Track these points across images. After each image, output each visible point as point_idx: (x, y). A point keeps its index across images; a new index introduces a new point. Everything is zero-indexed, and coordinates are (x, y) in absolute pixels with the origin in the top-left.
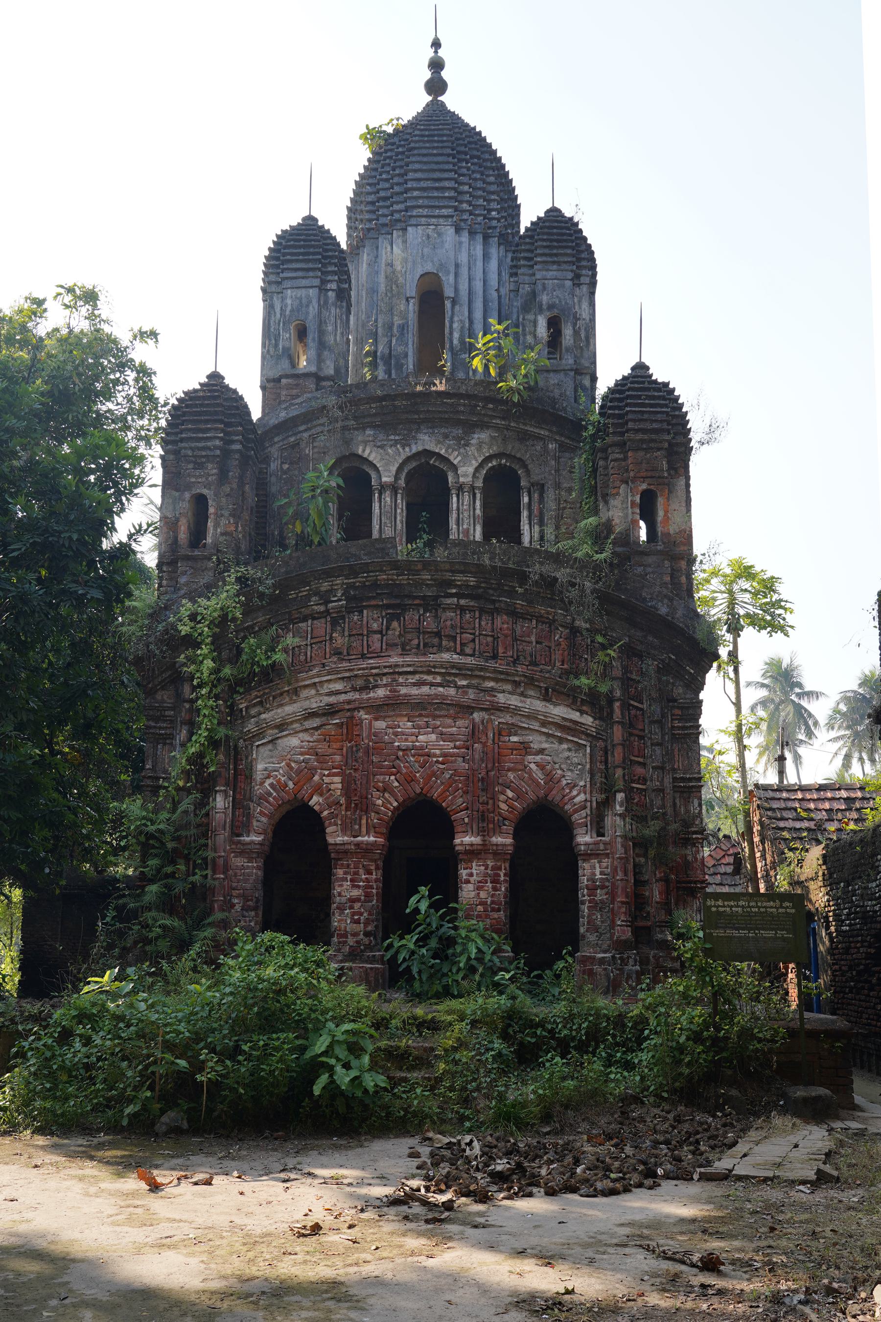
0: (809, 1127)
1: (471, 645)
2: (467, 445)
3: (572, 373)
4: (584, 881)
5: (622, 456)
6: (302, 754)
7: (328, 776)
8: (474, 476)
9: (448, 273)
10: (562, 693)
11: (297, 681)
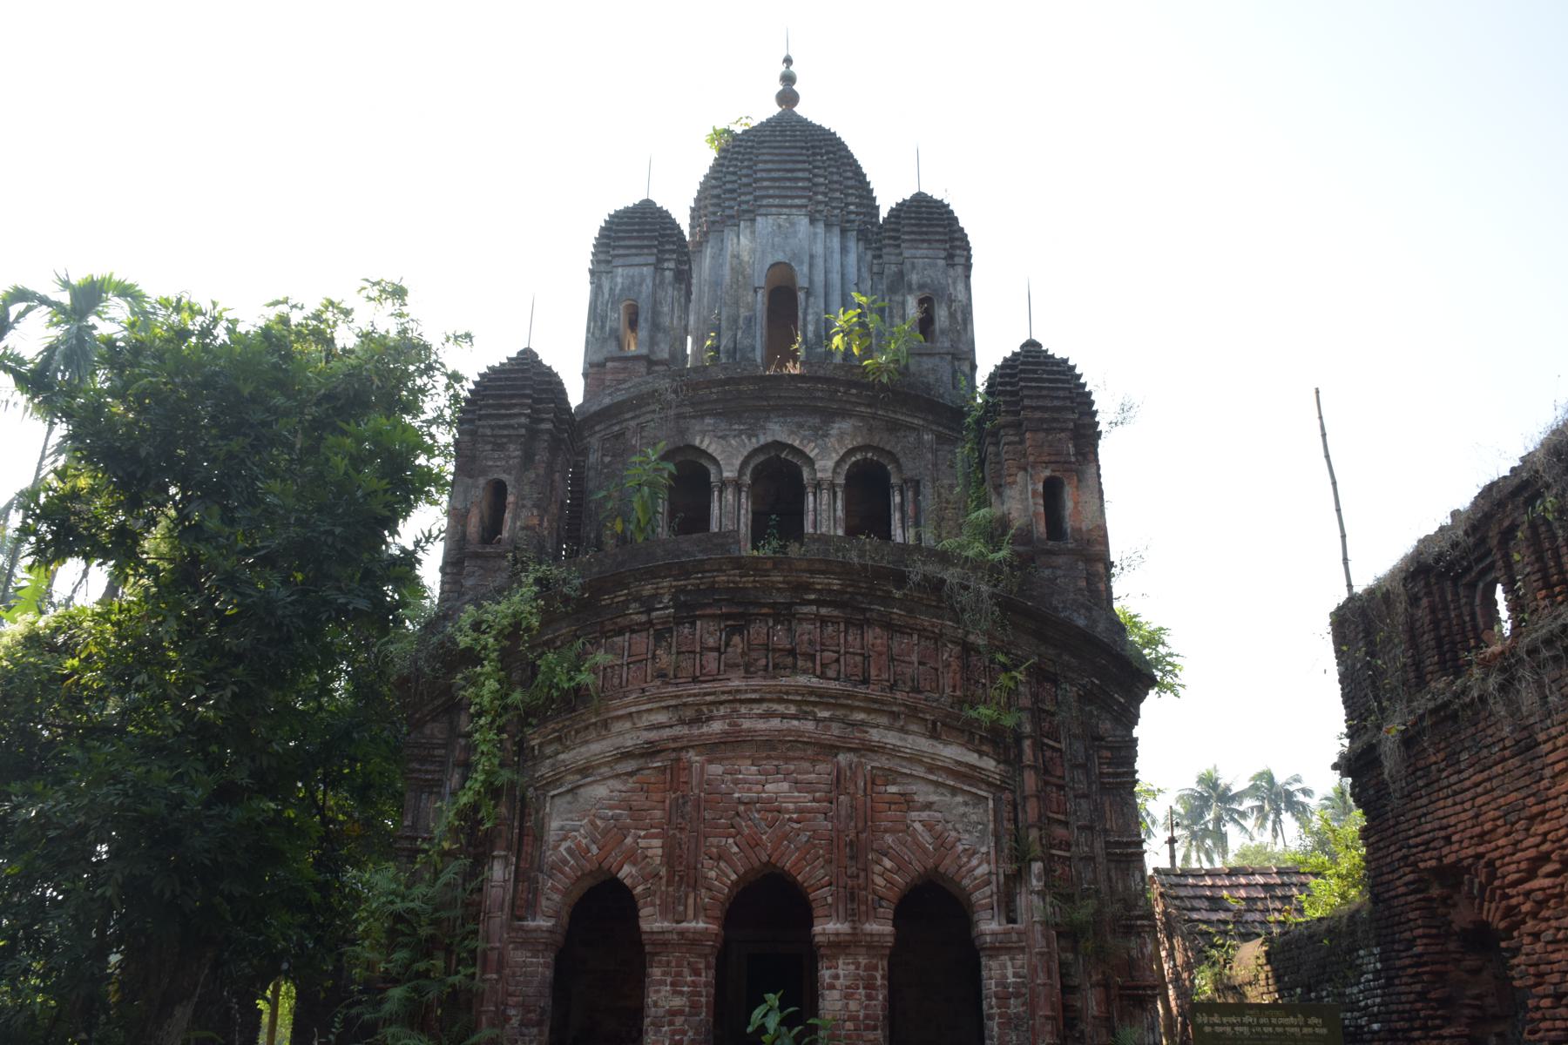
1: (835, 666)
2: (826, 435)
4: (990, 986)
6: (611, 808)
7: (644, 837)
8: (834, 471)
9: (802, 263)
10: (954, 728)
11: (608, 710)
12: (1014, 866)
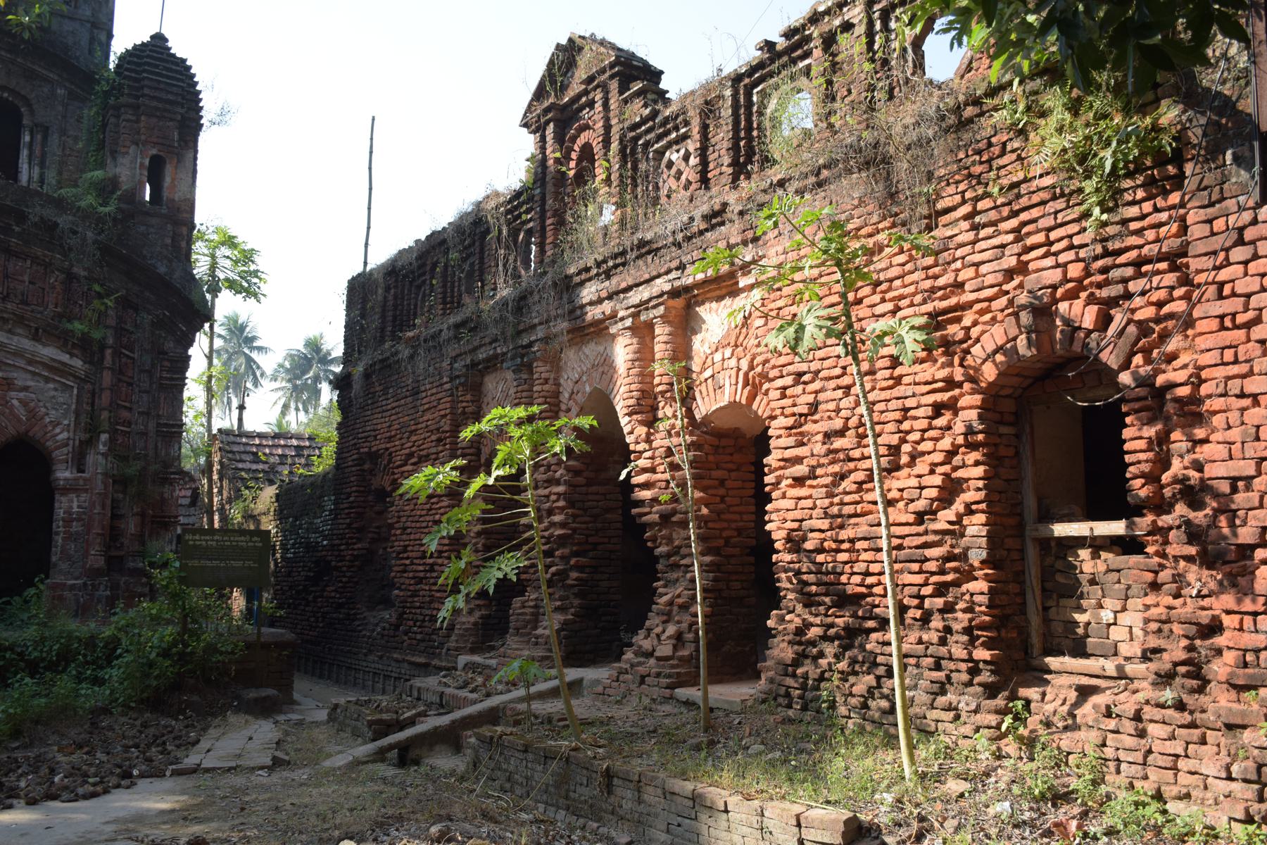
0: (259, 722)
3: (89, 25)
4: (60, 513)
5: (134, 118)
12: (88, 436)
